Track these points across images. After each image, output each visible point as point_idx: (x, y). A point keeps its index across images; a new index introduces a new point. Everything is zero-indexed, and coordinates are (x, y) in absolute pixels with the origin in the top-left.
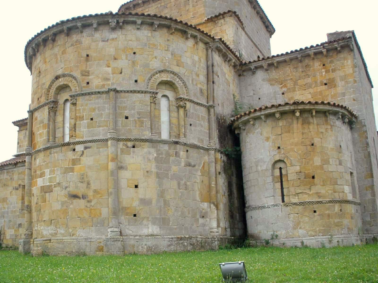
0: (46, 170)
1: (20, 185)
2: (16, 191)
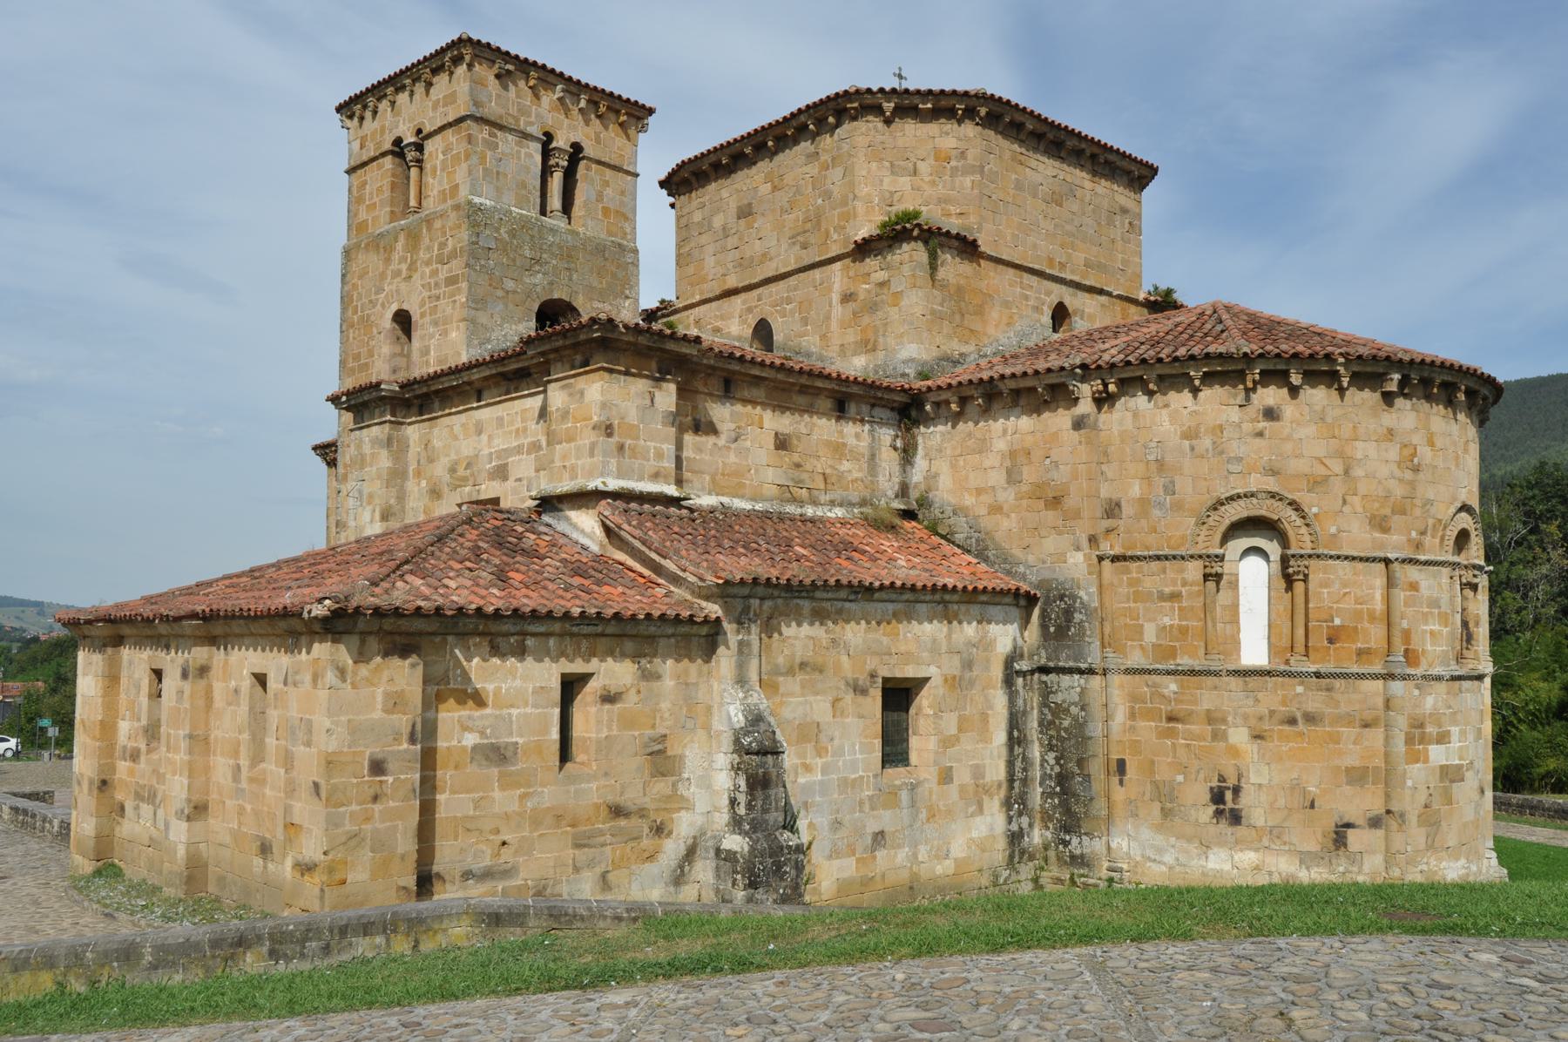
0: (1452, 729)
1: (873, 676)
2: (860, 699)
